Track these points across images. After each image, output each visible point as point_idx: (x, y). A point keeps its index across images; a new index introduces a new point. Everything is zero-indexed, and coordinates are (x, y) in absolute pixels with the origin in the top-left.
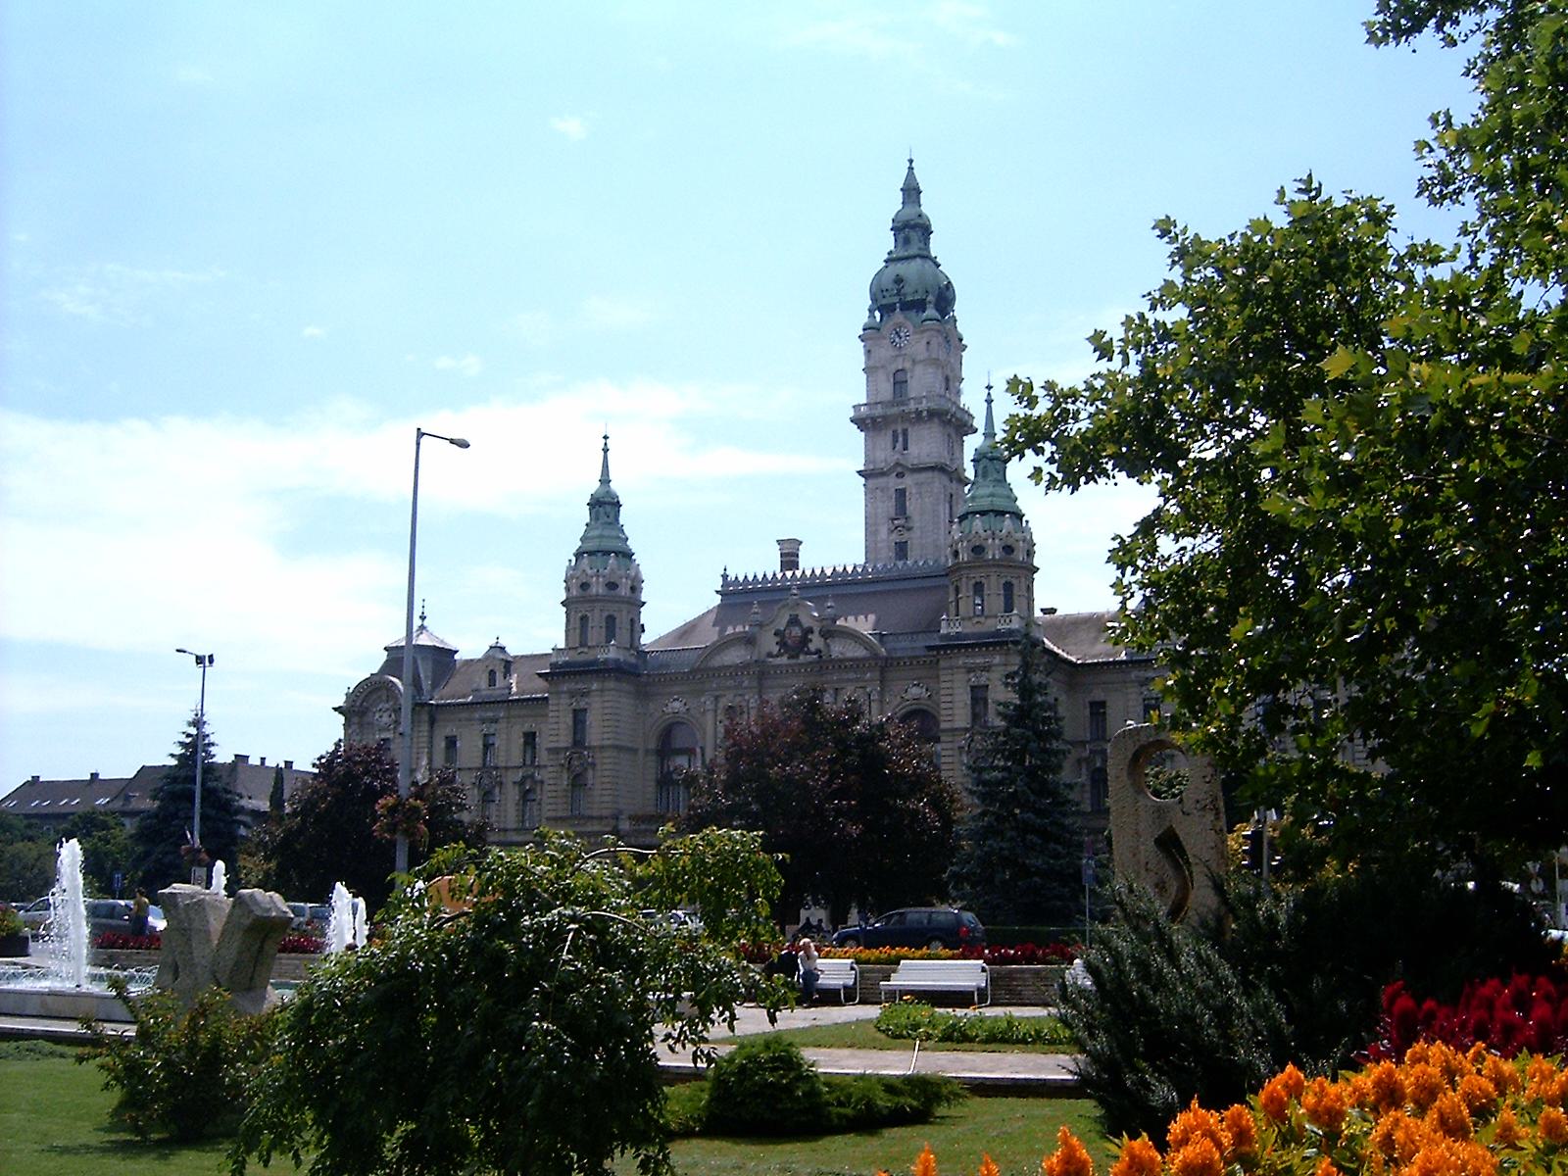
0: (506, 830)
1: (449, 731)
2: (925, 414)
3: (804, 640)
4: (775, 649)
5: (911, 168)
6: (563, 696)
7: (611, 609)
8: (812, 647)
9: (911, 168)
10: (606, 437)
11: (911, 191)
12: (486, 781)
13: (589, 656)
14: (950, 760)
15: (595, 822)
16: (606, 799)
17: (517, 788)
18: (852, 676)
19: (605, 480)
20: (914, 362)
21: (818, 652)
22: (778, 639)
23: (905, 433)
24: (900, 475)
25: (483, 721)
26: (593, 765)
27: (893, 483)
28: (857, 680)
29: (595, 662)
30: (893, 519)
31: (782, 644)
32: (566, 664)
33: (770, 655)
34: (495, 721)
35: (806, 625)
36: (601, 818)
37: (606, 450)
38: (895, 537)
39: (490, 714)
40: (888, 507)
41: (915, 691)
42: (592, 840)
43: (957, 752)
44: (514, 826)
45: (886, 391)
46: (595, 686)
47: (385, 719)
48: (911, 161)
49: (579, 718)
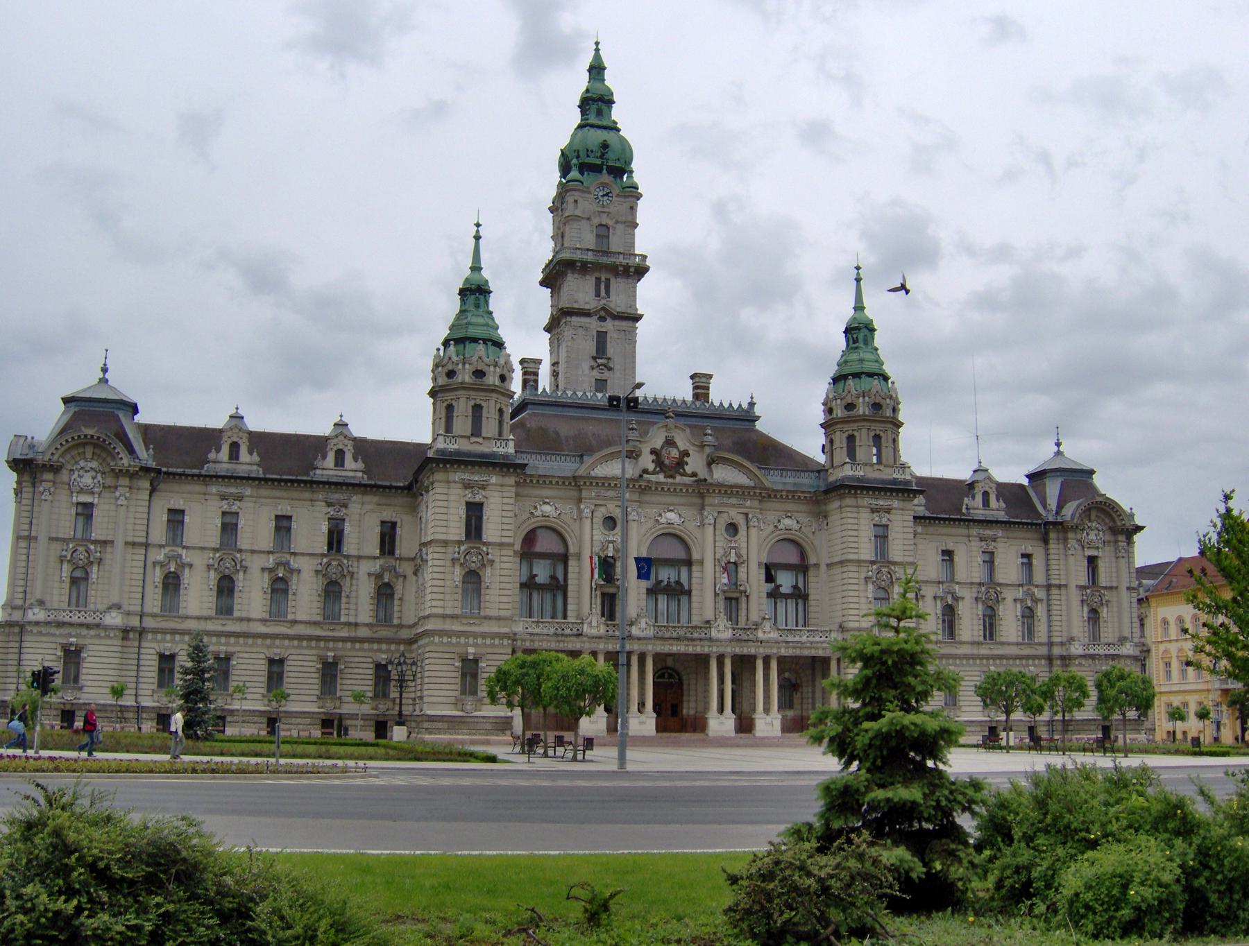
0: (249, 620)
1: (178, 503)
2: (632, 270)
3: (680, 464)
4: (651, 467)
5: (597, 50)
7: (478, 398)
8: (688, 469)
9: (597, 50)
10: (478, 225)
12: (332, 570)
14: (856, 587)
15: (493, 622)
18: (734, 501)
19: (476, 268)
21: (694, 474)
23: (608, 280)
24: (602, 319)
25: (223, 497)
26: (492, 562)
28: (739, 506)
29: (493, 455)
30: (594, 358)
31: (659, 462)
32: (458, 453)
33: (645, 471)
34: (240, 498)
36: (499, 619)
37: (477, 238)
38: (595, 373)
39: (232, 490)
40: (590, 347)
41: (787, 522)
45: (588, 239)
47: (87, 480)
48: (597, 44)
49: (475, 512)
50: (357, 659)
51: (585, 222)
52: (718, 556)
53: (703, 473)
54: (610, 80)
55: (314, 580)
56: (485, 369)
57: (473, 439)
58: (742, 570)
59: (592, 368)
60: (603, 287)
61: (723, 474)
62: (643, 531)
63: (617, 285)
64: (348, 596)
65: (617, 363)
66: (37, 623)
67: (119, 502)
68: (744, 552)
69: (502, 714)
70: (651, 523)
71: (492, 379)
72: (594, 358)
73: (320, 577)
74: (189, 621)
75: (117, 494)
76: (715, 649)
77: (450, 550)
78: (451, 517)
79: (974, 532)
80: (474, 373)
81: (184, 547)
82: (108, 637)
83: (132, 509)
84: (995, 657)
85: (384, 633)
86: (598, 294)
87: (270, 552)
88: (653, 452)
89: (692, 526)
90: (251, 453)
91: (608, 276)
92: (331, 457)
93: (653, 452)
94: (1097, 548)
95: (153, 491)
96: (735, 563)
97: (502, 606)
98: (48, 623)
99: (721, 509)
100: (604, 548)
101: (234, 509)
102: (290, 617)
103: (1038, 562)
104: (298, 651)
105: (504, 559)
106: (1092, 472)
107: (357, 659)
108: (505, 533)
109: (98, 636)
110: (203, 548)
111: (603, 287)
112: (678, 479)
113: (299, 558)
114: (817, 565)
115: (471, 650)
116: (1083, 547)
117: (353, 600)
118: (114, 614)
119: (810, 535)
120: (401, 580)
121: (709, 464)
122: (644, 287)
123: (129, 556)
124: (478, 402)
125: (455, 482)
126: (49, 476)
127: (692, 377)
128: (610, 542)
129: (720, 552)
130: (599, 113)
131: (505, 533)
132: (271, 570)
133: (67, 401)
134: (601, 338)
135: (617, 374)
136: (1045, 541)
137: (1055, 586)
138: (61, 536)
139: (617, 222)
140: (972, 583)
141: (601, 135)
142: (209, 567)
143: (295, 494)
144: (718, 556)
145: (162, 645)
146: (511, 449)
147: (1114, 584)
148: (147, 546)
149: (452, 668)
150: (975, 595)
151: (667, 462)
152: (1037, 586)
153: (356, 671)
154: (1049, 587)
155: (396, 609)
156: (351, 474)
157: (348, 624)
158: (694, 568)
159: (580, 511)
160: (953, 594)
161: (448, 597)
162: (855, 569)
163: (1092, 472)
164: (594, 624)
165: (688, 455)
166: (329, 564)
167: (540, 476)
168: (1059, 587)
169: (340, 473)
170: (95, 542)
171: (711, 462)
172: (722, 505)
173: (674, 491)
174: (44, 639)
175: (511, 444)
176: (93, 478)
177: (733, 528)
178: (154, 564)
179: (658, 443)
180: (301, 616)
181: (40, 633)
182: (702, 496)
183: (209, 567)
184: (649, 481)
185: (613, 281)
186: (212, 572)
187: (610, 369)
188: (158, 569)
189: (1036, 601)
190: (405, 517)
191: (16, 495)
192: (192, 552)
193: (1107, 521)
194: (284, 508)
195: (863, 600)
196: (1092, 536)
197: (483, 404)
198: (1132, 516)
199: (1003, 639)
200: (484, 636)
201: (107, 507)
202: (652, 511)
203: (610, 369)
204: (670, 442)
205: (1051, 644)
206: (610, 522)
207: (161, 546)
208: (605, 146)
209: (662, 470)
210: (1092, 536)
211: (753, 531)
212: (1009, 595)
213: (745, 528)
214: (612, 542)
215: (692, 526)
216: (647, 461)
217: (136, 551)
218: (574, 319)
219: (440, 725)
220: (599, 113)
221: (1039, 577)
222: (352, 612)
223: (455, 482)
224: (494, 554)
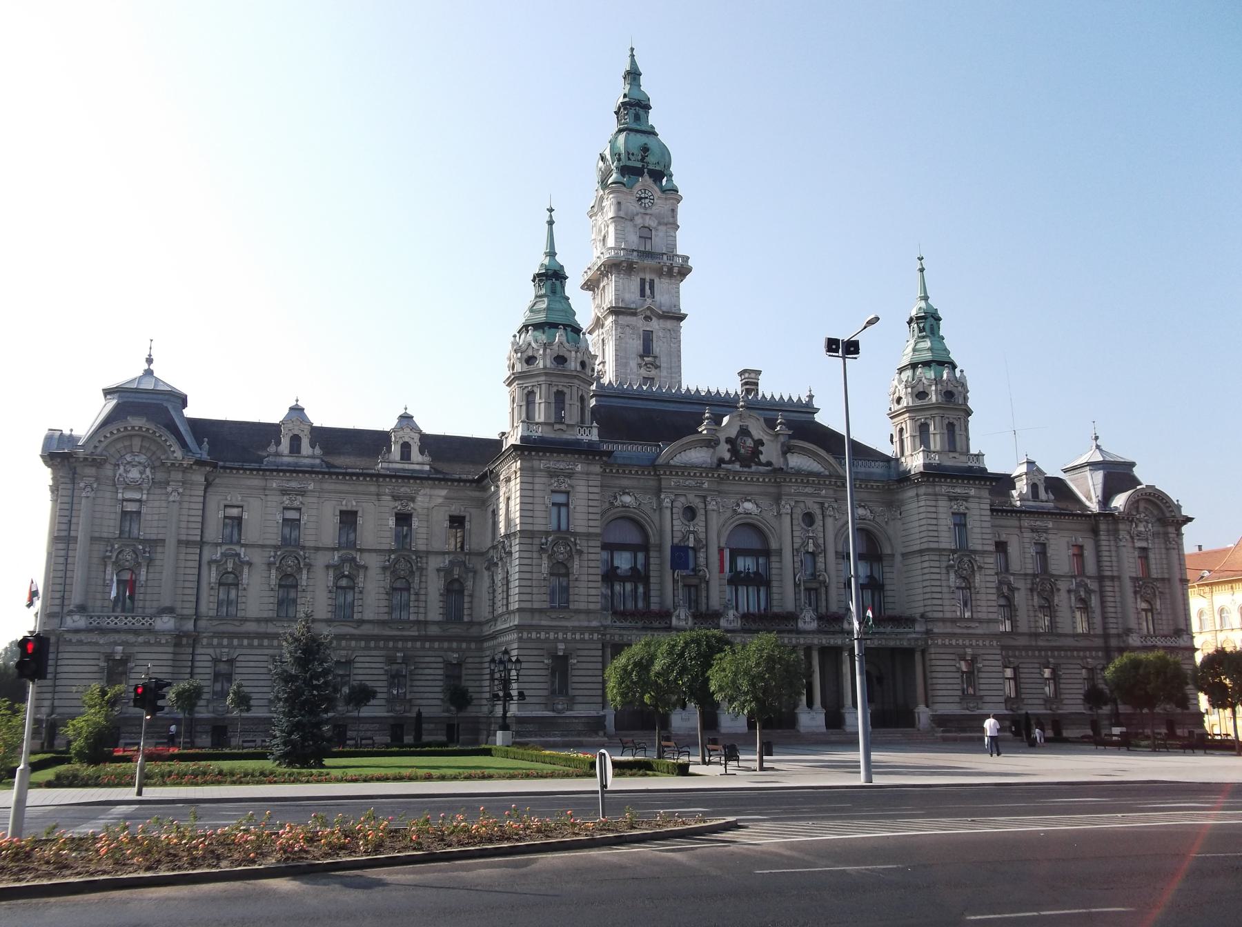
2: (676, 270)
3: (756, 453)
4: (727, 456)
5: (632, 56)
6: (539, 474)
8: (763, 458)
9: (632, 56)
10: (551, 210)
11: (633, 75)
13: (568, 436)
15: (582, 616)
16: (593, 592)
17: (331, 573)
18: (809, 490)
19: (552, 254)
20: (659, 224)
21: (769, 464)
24: (647, 318)
25: (284, 492)
27: (639, 322)
29: (578, 442)
31: (734, 451)
33: (721, 461)
34: (302, 493)
35: (756, 437)
37: (551, 223)
38: (643, 372)
39: (294, 484)
40: (637, 345)
42: (525, 635)
43: (944, 571)
44: (324, 617)
45: (633, 240)
46: (579, 468)
47: (134, 474)
48: (632, 49)
50: (427, 659)
51: (629, 223)
52: (796, 546)
53: (778, 462)
54: (646, 85)
55: (381, 577)
56: (566, 355)
57: (557, 427)
58: (820, 559)
59: (640, 366)
60: (647, 287)
61: (795, 461)
62: (722, 521)
63: (661, 285)
64: (417, 594)
65: (664, 361)
66: (77, 631)
67: (171, 499)
68: (821, 541)
69: (594, 713)
70: (729, 513)
71: (573, 365)
72: (642, 357)
73: (388, 573)
74: (248, 624)
75: (169, 489)
76: (802, 641)
77: (536, 541)
78: (537, 507)
79: (1025, 523)
80: (555, 359)
81: (243, 546)
82: (159, 644)
83: (186, 505)
84: (1053, 649)
85: (455, 630)
86: (643, 294)
87: (334, 549)
88: (728, 440)
89: (769, 515)
90: (313, 446)
91: (653, 277)
92: (395, 449)
93: (728, 440)
94: (1147, 540)
95: (208, 484)
96: (813, 554)
97: (591, 599)
98: (88, 630)
99: (797, 498)
100: (685, 538)
101: (296, 504)
102: (356, 616)
103: (1089, 553)
104: (367, 653)
105: (591, 550)
106: (1133, 464)
107: (427, 659)
108: (591, 523)
109: (147, 643)
110: (263, 546)
111: (647, 287)
112: (754, 468)
113: (366, 555)
114: (893, 555)
115: (561, 646)
116: (1132, 538)
117: (422, 598)
118: (165, 619)
119: (883, 524)
120: (471, 575)
121: (784, 453)
122: (686, 286)
123: (182, 556)
124: (560, 388)
125: (540, 470)
126: (91, 471)
127: (741, 374)
128: (690, 532)
129: (798, 541)
130: (637, 118)
131: (591, 523)
132: (336, 567)
133: (108, 392)
134: (648, 338)
135: (664, 373)
136: (1095, 532)
137: (1107, 577)
138: (105, 535)
139: (659, 224)
140: (1026, 575)
141: (641, 139)
142: (269, 565)
143: (360, 488)
144: (796, 546)
145: (218, 651)
146: (594, 436)
147: (1166, 576)
148: (202, 544)
149: (541, 666)
150: (1029, 586)
151: (742, 451)
152: (1089, 577)
153: (427, 671)
154: (1101, 578)
155: (466, 606)
156: (417, 467)
157: (418, 622)
158: (773, 559)
159: (660, 502)
160: (1009, 584)
161: (535, 590)
162: (937, 558)
163: (1133, 464)
164: (683, 616)
165: (763, 444)
166: (397, 561)
167: (620, 465)
168: (1112, 578)
169: (406, 466)
170: (145, 541)
171: (787, 450)
174: (85, 648)
175: (595, 431)
176: (141, 473)
177: (809, 518)
178: (210, 563)
180: (369, 615)
181: (80, 642)
182: (778, 485)
183: (269, 565)
184: (728, 470)
185: (656, 281)
186: (273, 572)
187: (657, 367)
188: (214, 569)
189: (1089, 592)
190: (473, 511)
191: (52, 492)
192: (249, 550)
193: (1155, 512)
194: (350, 504)
195: (945, 590)
196: (1141, 528)
197: (565, 390)
198: (1179, 507)
199: (1060, 631)
200: (574, 630)
201: (157, 504)
202: (731, 502)
203: (657, 367)
204: (744, 432)
205: (1106, 636)
206: (690, 513)
207: (217, 545)
208: (645, 149)
209: (737, 459)
210: (1141, 528)
211: (829, 521)
212: (1063, 585)
213: (820, 517)
214: (693, 532)
215: (769, 515)
216: (724, 451)
217: (190, 550)
219: (531, 727)
220: (637, 118)
221: (1091, 568)
222: (422, 610)
223: (540, 470)
224: (582, 544)
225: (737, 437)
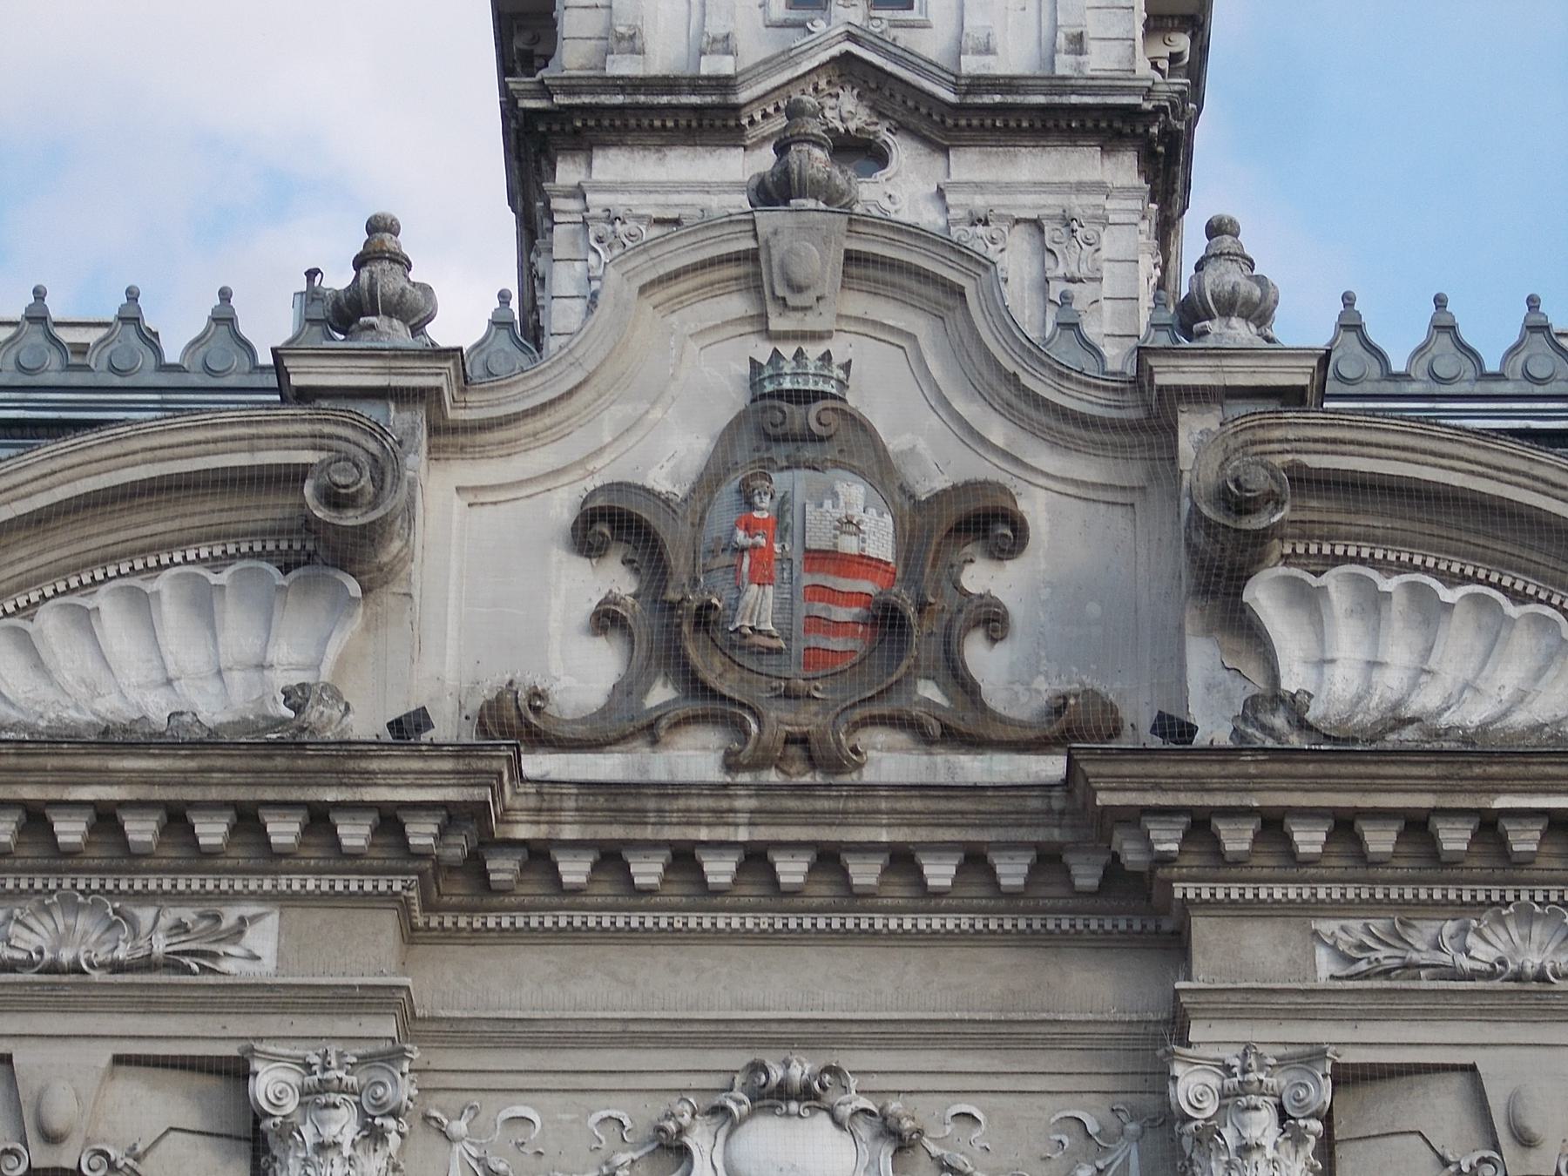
3: (905, 629)
4: (584, 675)
21: (1074, 726)
22: (613, 578)
33: (515, 723)
88: (610, 524)
93: (610, 524)
151: (760, 607)
165: (989, 523)
172: (1388, 989)
173: (835, 891)
179: (666, 451)
182: (1144, 918)
204: (787, 423)
209: (706, 704)
218: (612, 165)
225: (708, 481)
